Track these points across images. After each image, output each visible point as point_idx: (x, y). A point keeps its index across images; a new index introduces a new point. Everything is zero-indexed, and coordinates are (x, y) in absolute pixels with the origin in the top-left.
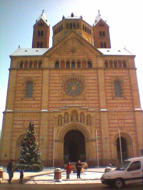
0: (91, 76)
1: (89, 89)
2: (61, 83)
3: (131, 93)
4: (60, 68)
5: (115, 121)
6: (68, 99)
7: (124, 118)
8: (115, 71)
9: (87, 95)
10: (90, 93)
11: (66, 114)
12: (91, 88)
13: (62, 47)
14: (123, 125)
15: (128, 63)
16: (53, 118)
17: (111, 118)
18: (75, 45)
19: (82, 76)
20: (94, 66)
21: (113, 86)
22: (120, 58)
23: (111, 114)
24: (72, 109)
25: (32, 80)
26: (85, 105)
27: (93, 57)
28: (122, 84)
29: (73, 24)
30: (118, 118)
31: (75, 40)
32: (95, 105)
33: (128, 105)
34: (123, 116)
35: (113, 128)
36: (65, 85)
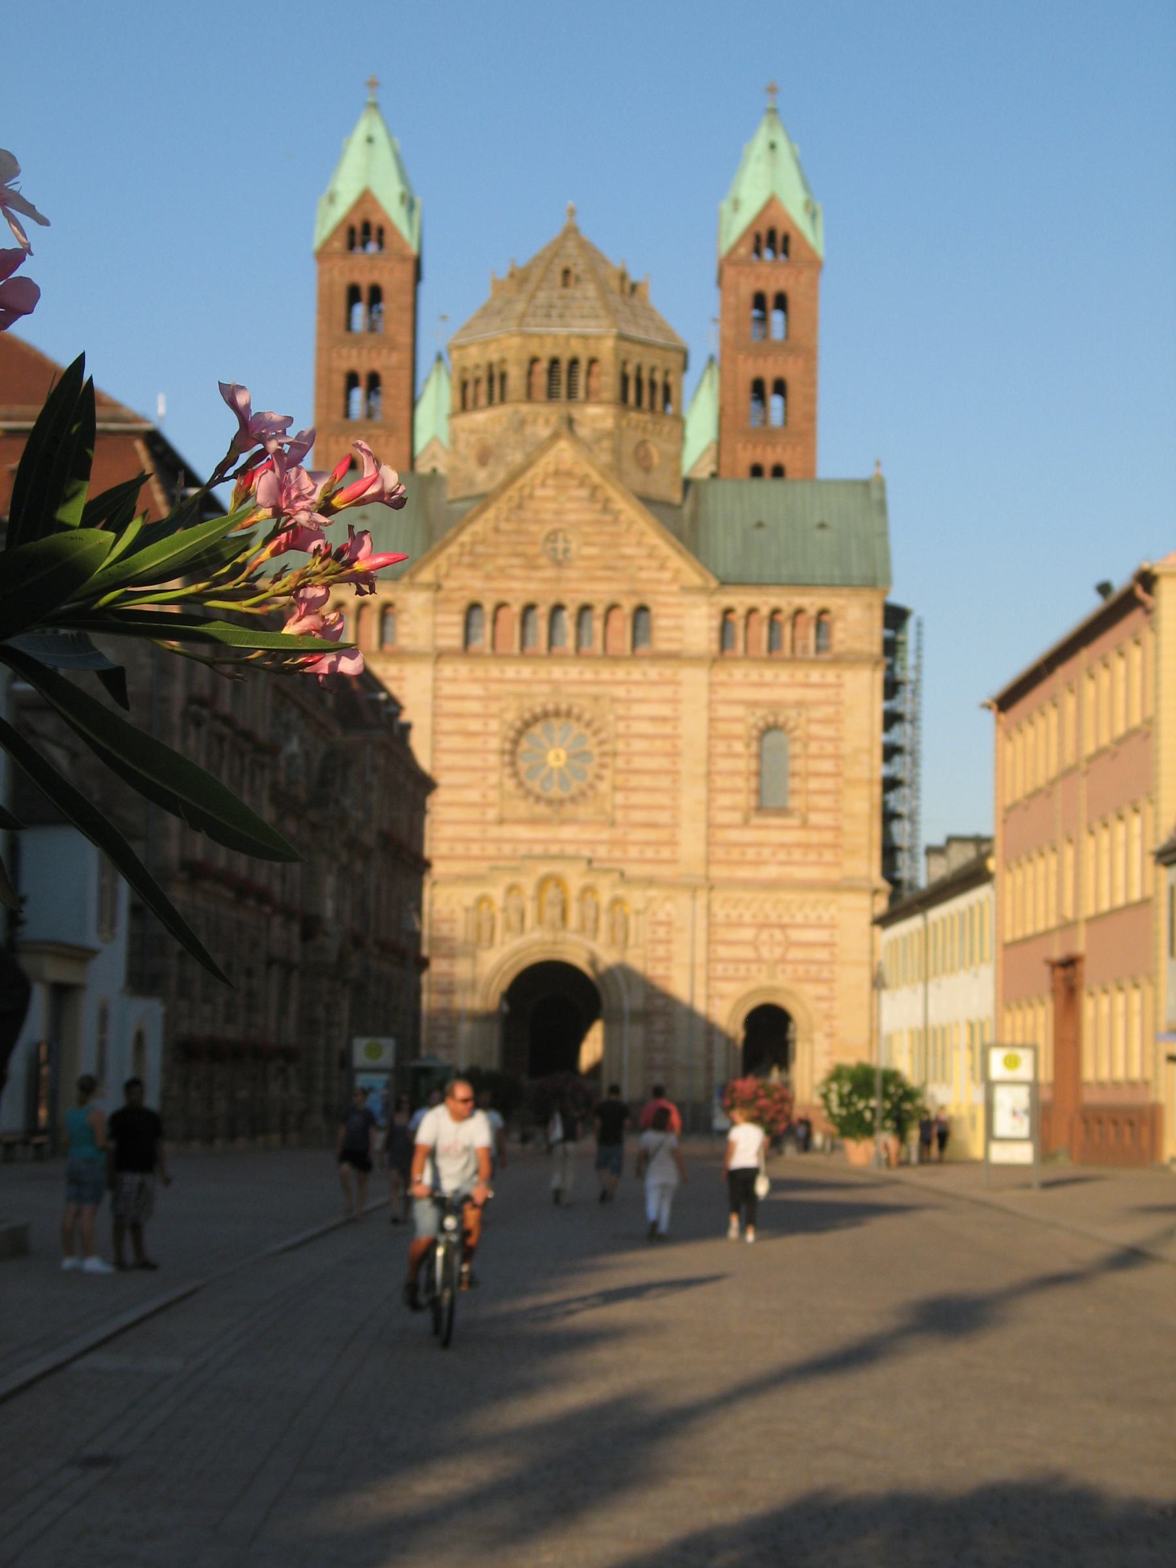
2: (493, 734)
7: (786, 920)
8: (769, 674)
9: (620, 798)
10: (635, 789)
12: (639, 763)
13: (504, 526)
14: (778, 952)
18: (572, 517)
19: (596, 698)
24: (544, 869)
33: (812, 857)
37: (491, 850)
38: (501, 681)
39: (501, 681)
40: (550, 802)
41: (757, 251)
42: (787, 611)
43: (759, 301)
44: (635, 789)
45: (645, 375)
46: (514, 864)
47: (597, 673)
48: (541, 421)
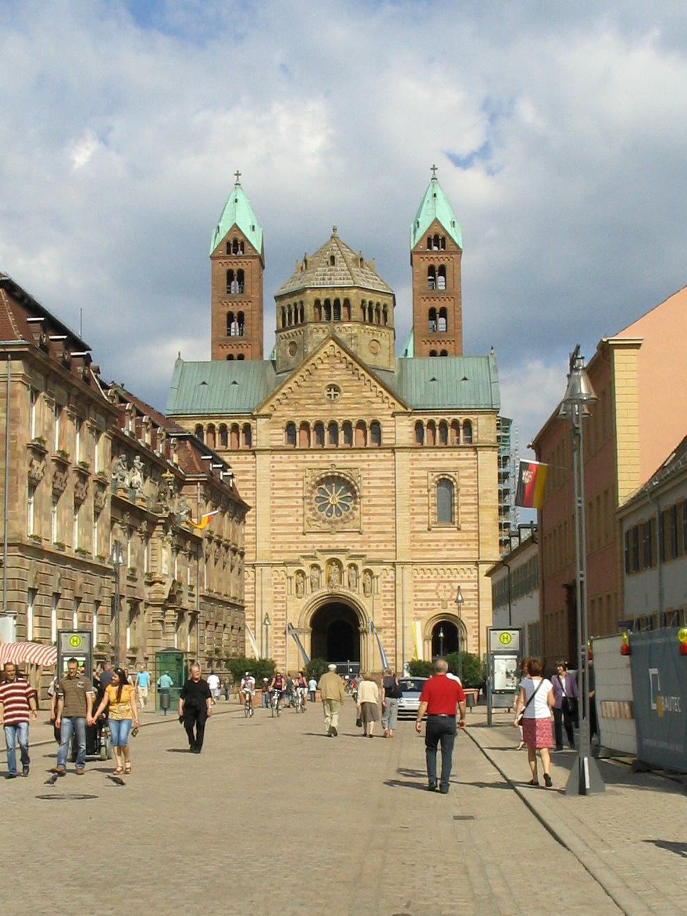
0: (377, 469)
1: (371, 503)
4: (297, 447)
5: (429, 584)
8: (439, 454)
9: (365, 519)
10: (373, 514)
11: (315, 568)
12: (375, 501)
13: (303, 384)
14: (449, 594)
15: (477, 431)
16: (283, 579)
17: (422, 577)
18: (338, 378)
20: (384, 442)
21: (433, 496)
23: (422, 569)
26: (358, 545)
27: (382, 415)
28: (455, 489)
29: (332, 303)
31: (339, 361)
34: (452, 573)
35: (425, 603)
36: (311, 492)
37: (301, 547)
38: (304, 462)
39: (304, 462)
40: (330, 522)
41: (429, 247)
42: (450, 422)
43: (431, 270)
44: (373, 514)
45: (374, 306)
46: (313, 554)
48: (321, 330)
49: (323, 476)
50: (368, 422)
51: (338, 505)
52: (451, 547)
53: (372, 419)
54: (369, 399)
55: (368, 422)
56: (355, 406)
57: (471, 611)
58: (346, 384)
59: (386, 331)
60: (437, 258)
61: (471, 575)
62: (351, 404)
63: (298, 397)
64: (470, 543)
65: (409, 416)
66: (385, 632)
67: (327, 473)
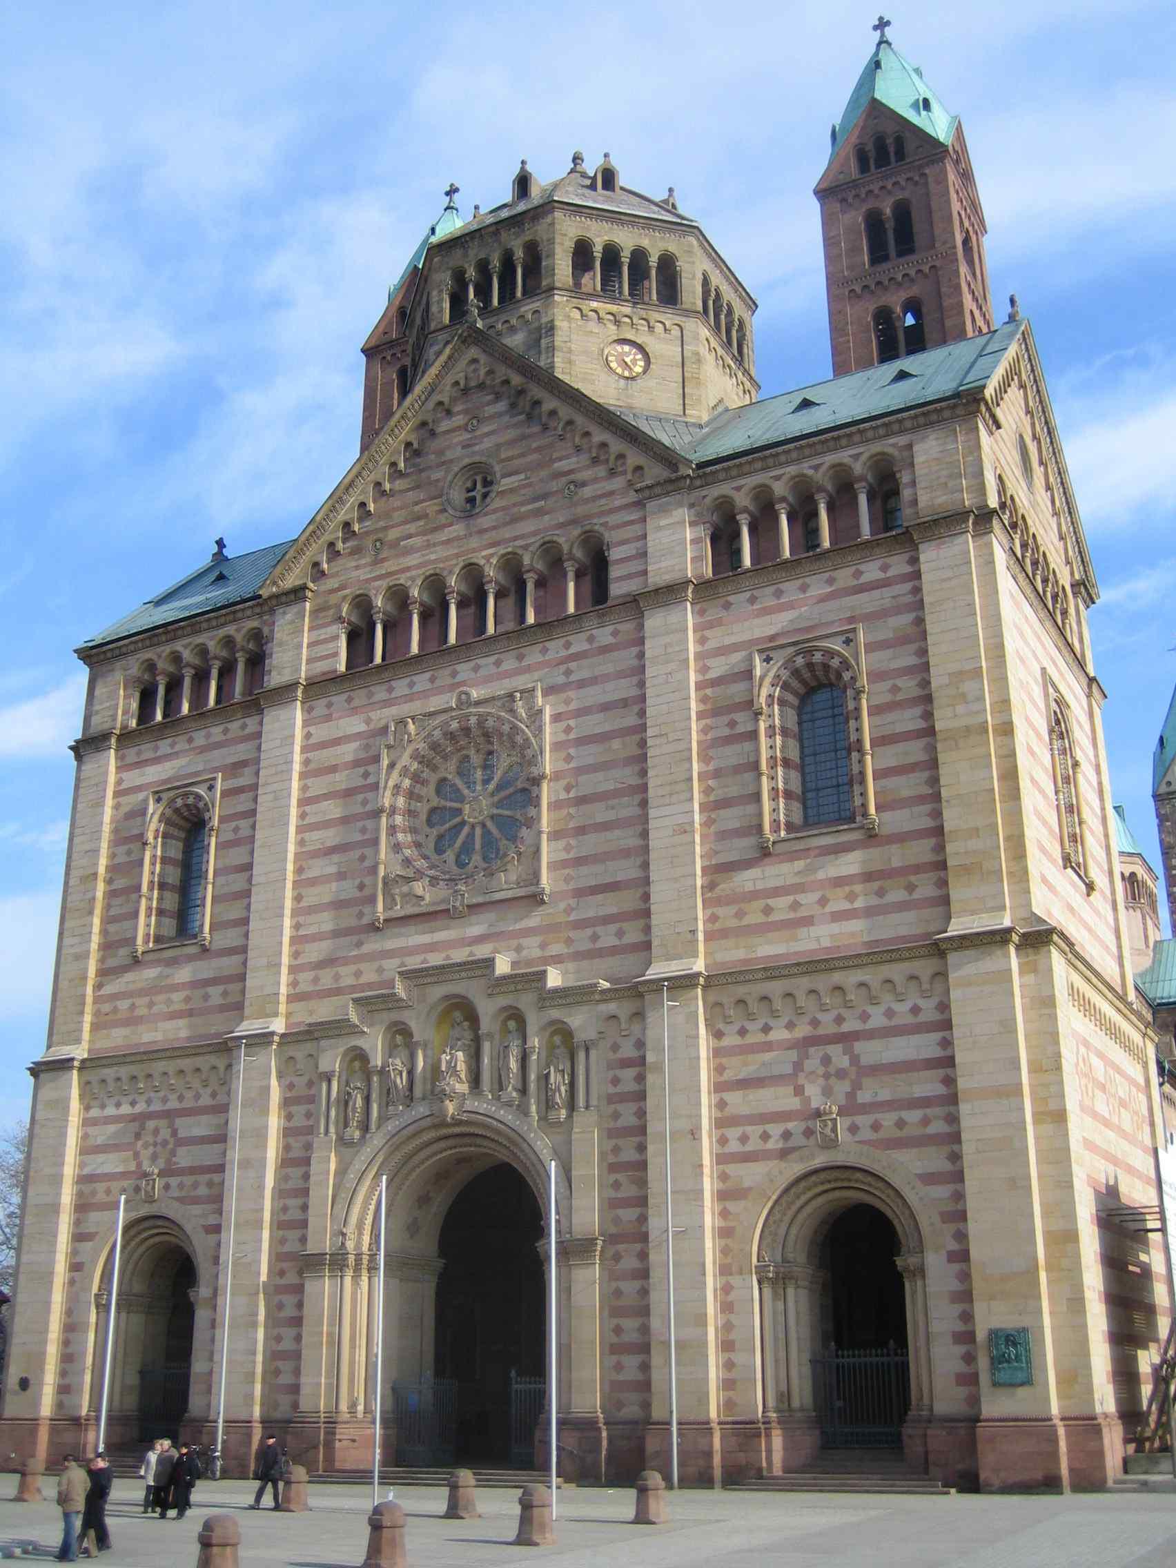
3: (933, 764)
6: (417, 910)
7: (850, 1025)
14: (842, 1088)
15: (913, 483)
16: (310, 1084)
18: (487, 443)
22: (844, 456)
23: (741, 1002)
24: (438, 992)
25: (198, 797)
27: (612, 511)
28: (850, 692)
30: (802, 1030)
32: (620, 934)
33: (897, 895)
35: (754, 1131)
47: (520, 658)
49: (437, 733)
50: (567, 540)
51: (489, 824)
52: (846, 906)
53: (576, 532)
54: (572, 477)
55: (567, 540)
56: (530, 507)
57: (931, 1150)
58: (510, 453)
59: (669, 317)
60: (883, 188)
61: (921, 1003)
62: (522, 504)
63: (382, 524)
64: (913, 878)
65: (692, 488)
66: (617, 1258)
67: (447, 723)
